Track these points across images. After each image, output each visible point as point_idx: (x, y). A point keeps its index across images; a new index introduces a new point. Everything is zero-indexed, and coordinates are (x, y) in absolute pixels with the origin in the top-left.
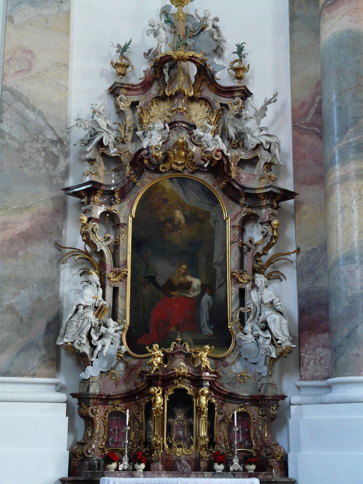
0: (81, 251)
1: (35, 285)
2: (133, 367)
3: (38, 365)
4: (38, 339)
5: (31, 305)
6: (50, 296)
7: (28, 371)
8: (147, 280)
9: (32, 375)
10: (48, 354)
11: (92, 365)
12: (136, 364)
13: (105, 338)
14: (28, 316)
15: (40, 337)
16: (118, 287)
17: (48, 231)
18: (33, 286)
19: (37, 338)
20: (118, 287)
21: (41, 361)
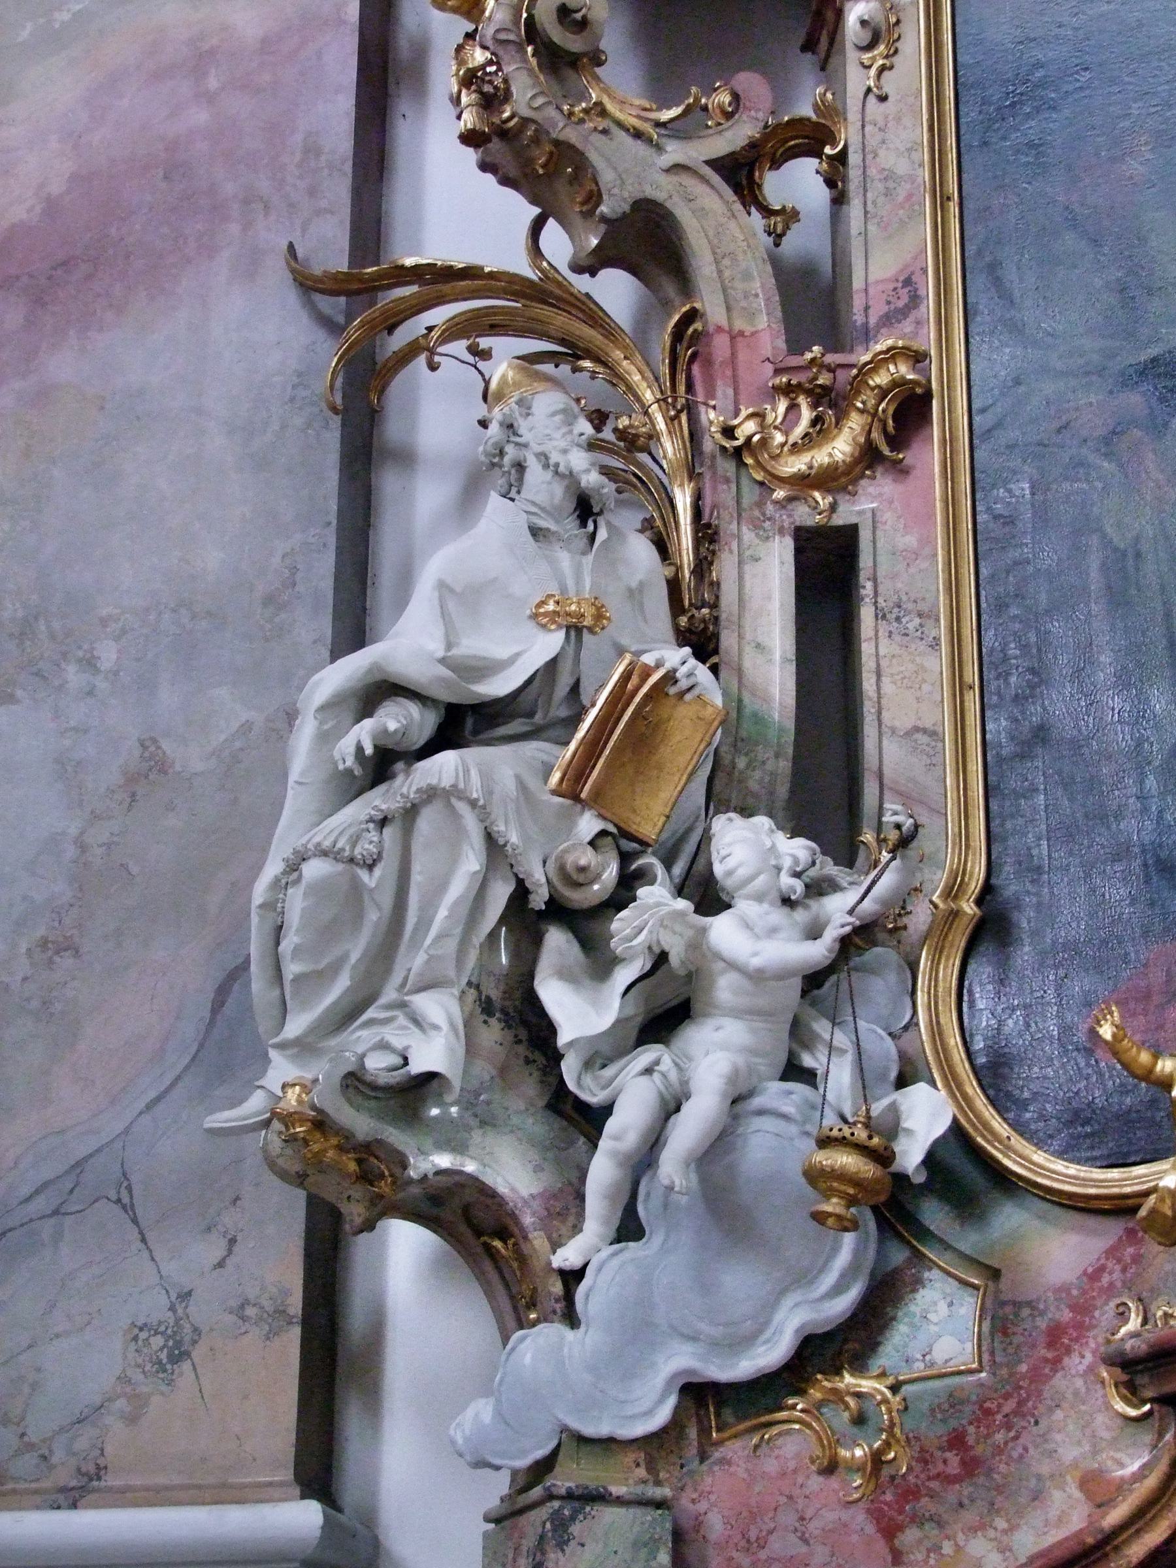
0: (492, 276)
1: (108, 654)
2: (1066, 1315)
3: (124, 1379)
4: (127, 1131)
5: (73, 831)
6: (247, 727)
7: (31, 1447)
8: (1135, 400)
9: (64, 1490)
10: (221, 1265)
11: (571, 1318)
12: (1094, 1275)
13: (706, 1015)
14: (41, 932)
15: (149, 1107)
16: (851, 532)
17: (229, 188)
18: (90, 663)
19: (120, 1127)
20: (851, 532)
21: (157, 1341)
